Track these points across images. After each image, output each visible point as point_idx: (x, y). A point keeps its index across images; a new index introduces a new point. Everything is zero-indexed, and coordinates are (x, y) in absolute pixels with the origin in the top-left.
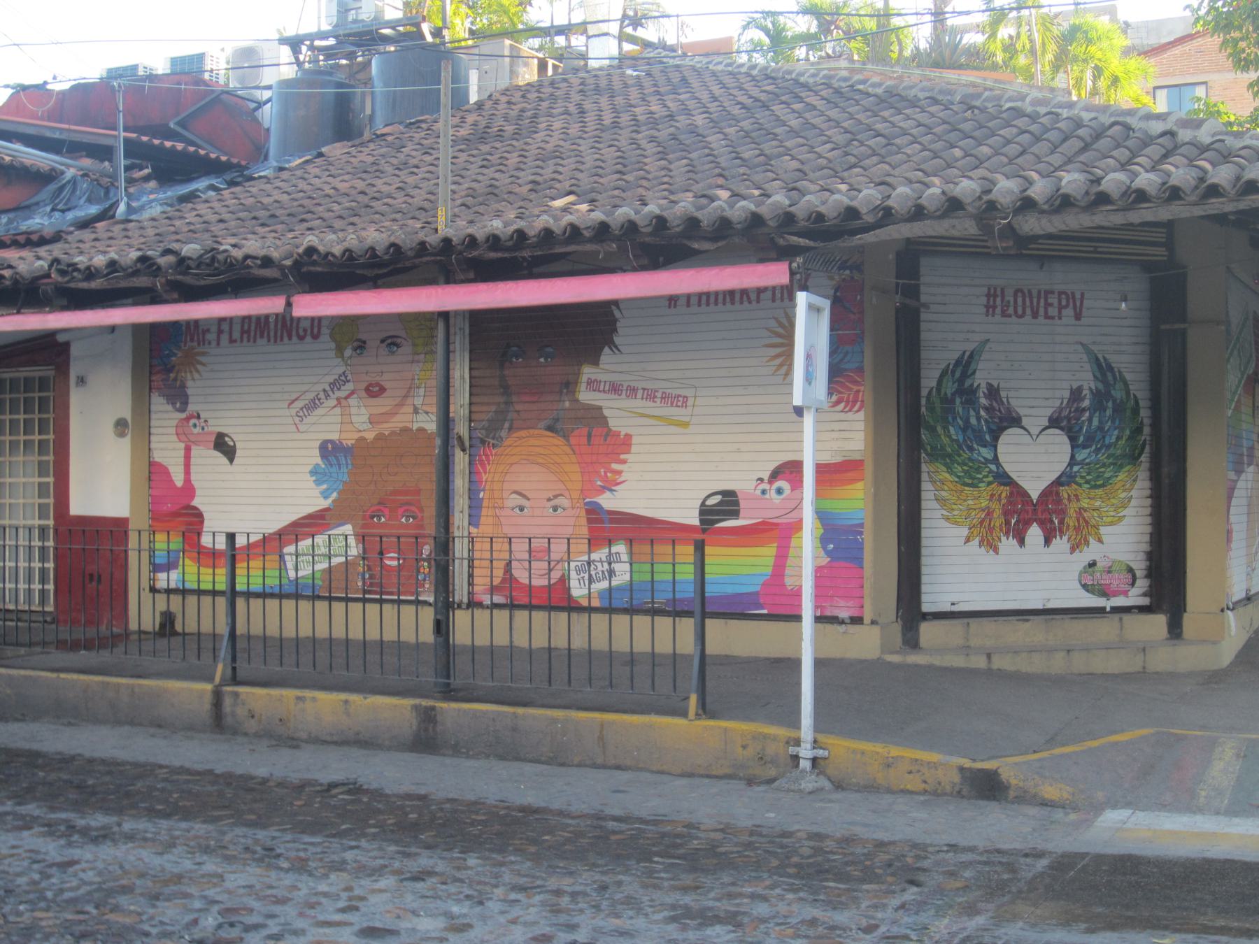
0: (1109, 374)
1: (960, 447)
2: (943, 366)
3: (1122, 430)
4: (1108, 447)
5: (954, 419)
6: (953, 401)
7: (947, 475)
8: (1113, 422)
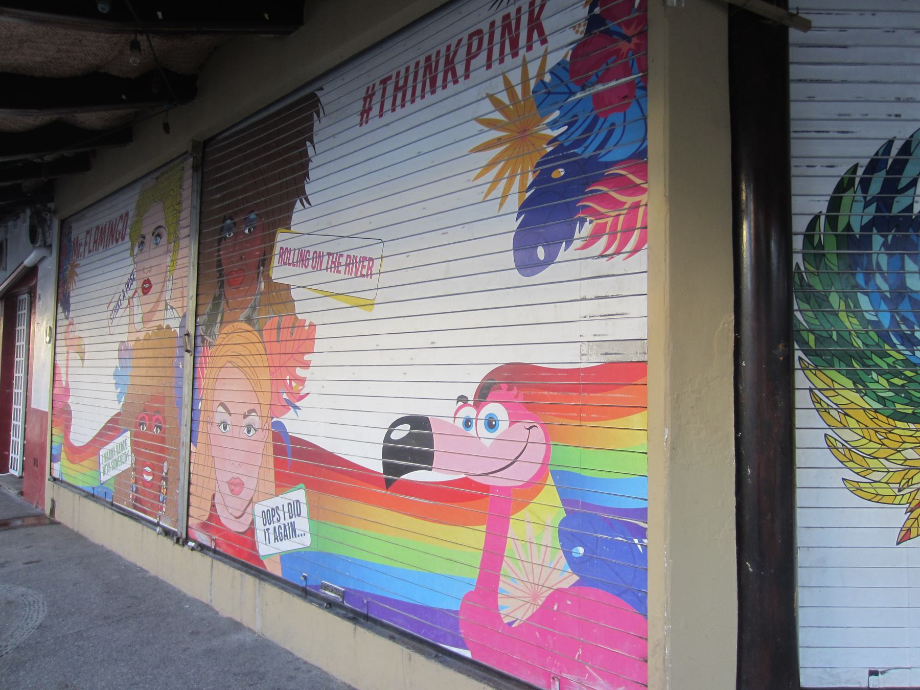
1: (884, 336)
2: (842, 170)
5: (869, 277)
6: (866, 242)
7: (855, 397)
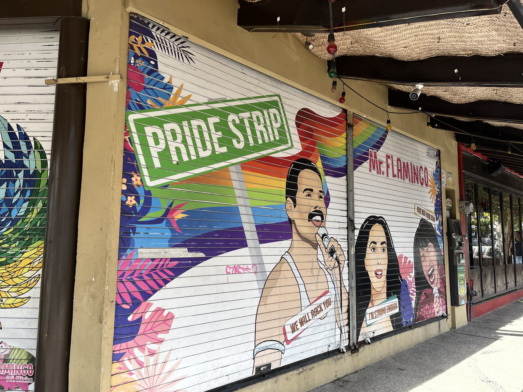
0: (22, 144)
3: (33, 203)
4: (14, 222)
8: (23, 193)
